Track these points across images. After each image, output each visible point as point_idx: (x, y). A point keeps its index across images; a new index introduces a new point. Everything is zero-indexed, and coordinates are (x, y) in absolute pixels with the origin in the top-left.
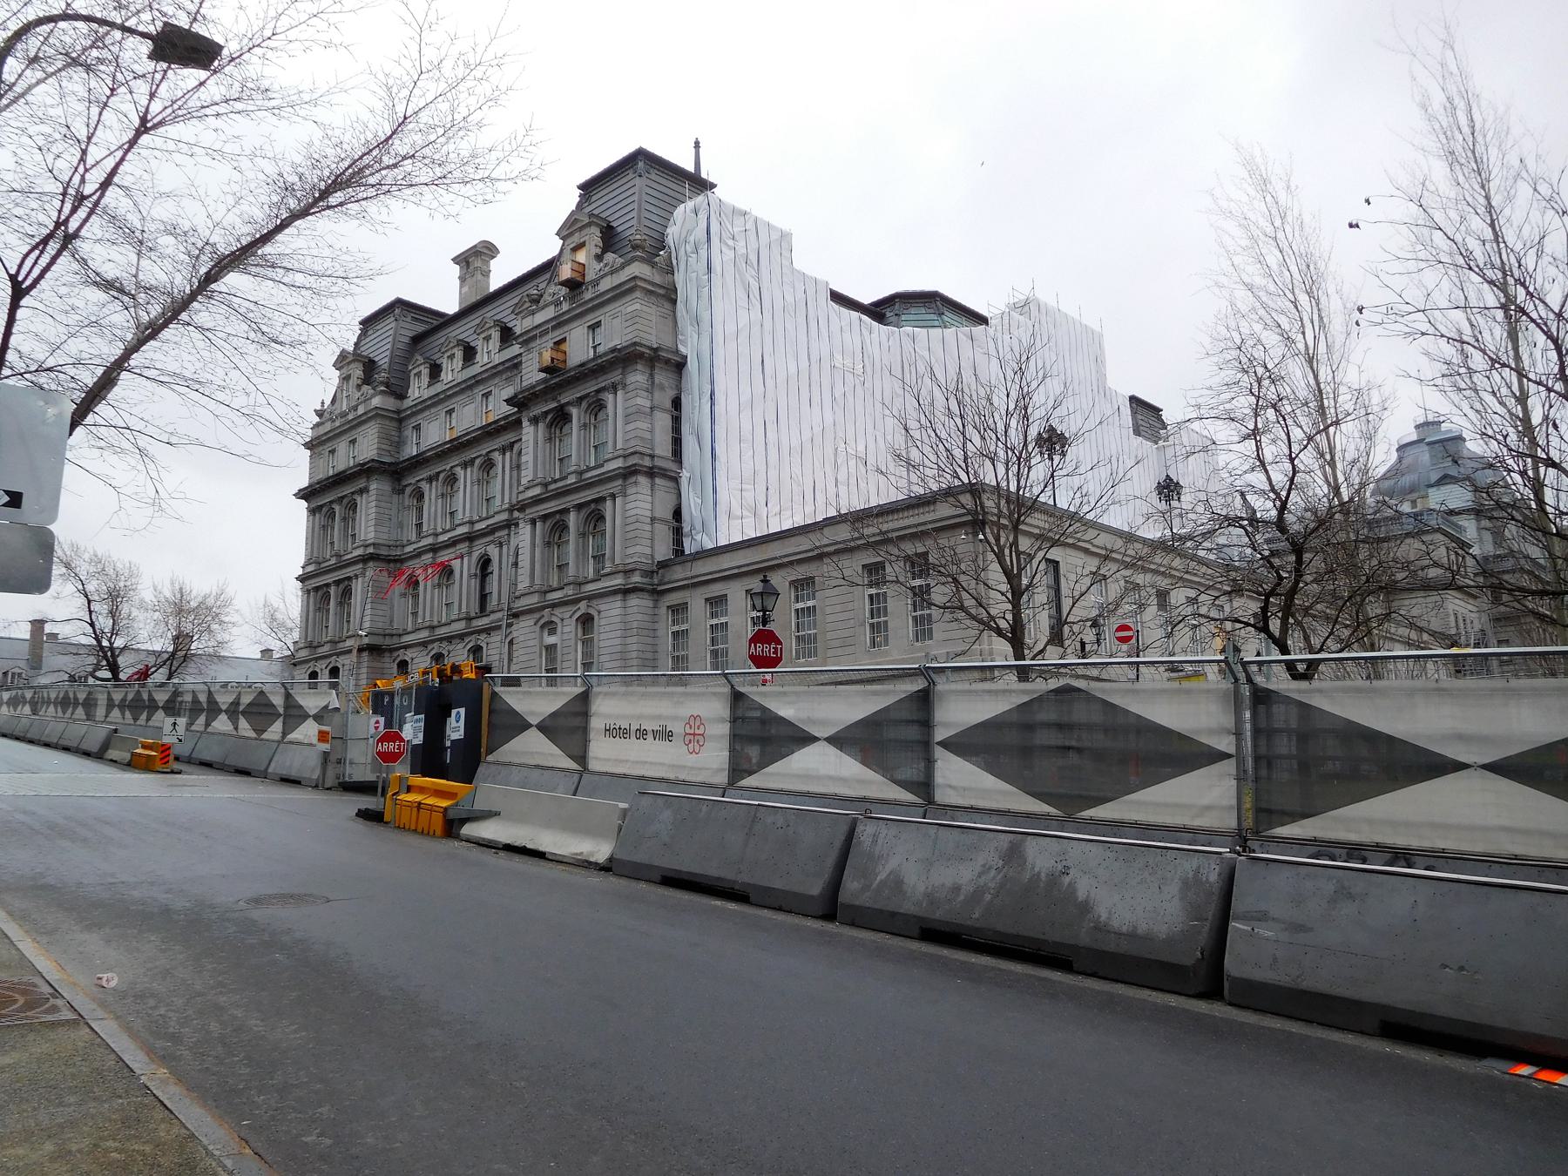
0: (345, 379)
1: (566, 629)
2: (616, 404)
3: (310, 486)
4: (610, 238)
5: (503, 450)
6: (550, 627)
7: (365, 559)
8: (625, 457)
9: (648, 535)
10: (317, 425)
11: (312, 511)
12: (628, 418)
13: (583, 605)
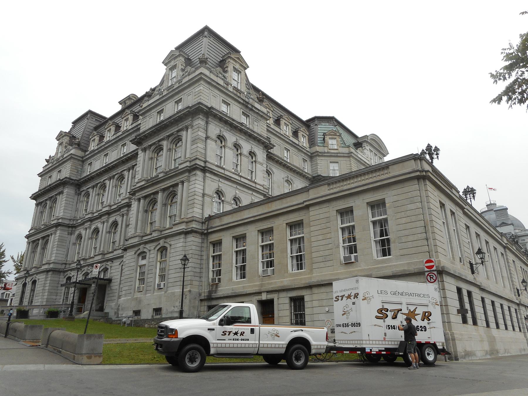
0: (60, 144)
1: (152, 256)
2: (187, 136)
3: (39, 191)
4: (188, 61)
5: (129, 170)
6: (143, 255)
7: (57, 225)
8: (190, 162)
9: (201, 203)
10: (46, 166)
11: (37, 205)
12: (194, 142)
13: (162, 242)
